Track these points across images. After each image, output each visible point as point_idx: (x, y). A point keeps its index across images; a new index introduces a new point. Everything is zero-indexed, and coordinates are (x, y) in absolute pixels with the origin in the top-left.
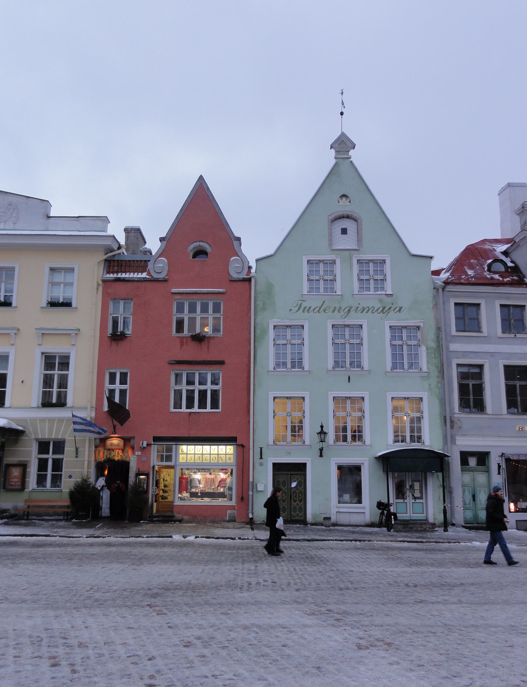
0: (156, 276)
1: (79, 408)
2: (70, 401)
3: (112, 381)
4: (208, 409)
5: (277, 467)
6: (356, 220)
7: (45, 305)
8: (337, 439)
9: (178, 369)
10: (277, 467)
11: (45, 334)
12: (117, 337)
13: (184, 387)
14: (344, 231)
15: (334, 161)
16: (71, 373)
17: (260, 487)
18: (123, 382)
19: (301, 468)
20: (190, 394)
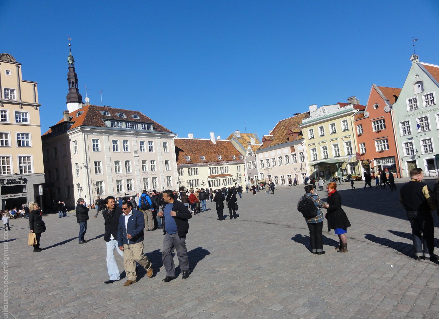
0: (366, 117)
4: (387, 149)
12: (360, 135)
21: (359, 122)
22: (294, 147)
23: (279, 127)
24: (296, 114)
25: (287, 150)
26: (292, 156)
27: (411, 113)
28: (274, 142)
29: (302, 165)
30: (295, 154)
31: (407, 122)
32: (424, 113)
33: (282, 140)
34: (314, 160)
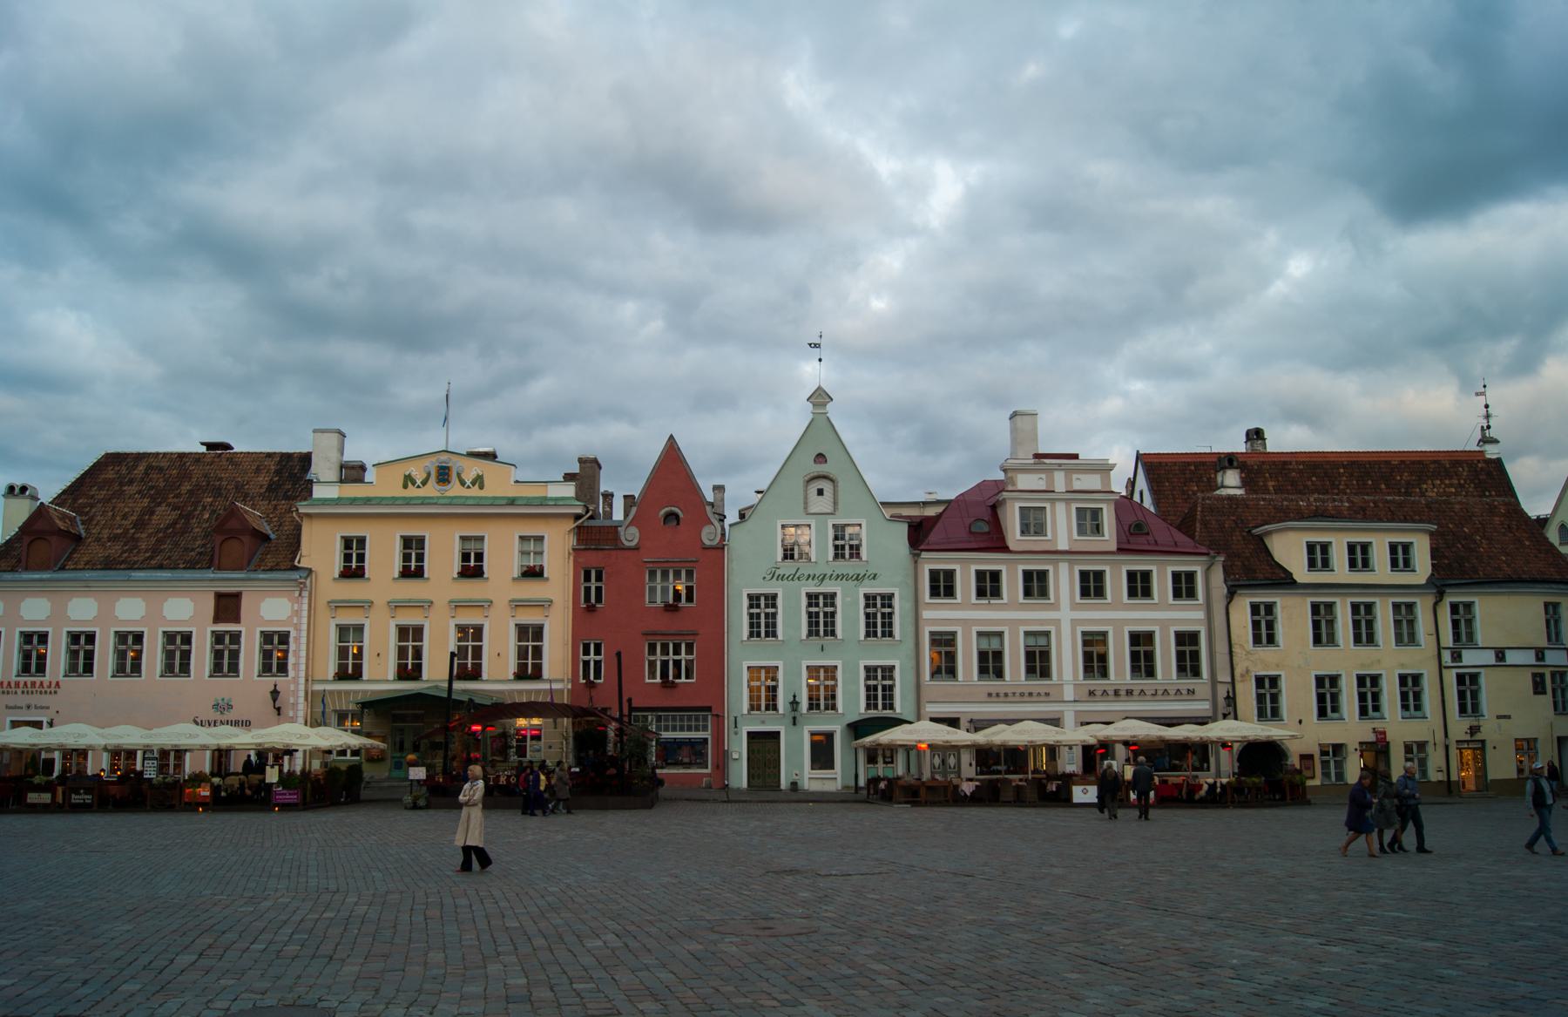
0: (627, 544)
1: (557, 681)
2: (546, 674)
3: (586, 652)
4: (683, 680)
5: (752, 736)
6: (832, 480)
7: (516, 573)
8: (811, 707)
9: (652, 639)
10: (752, 736)
11: (518, 605)
12: (591, 609)
13: (659, 657)
14: (820, 492)
15: (811, 416)
16: (546, 644)
17: (735, 756)
18: (598, 652)
19: (775, 735)
20: (665, 664)
21: (594, 559)
22: (237, 596)
23: (110, 482)
24: (210, 446)
25: (184, 607)
26: (209, 639)
27: (788, 568)
28: (100, 553)
29: (275, 694)
30: (235, 638)
31: (772, 599)
32: (827, 581)
33: (155, 551)
34: (342, 675)
